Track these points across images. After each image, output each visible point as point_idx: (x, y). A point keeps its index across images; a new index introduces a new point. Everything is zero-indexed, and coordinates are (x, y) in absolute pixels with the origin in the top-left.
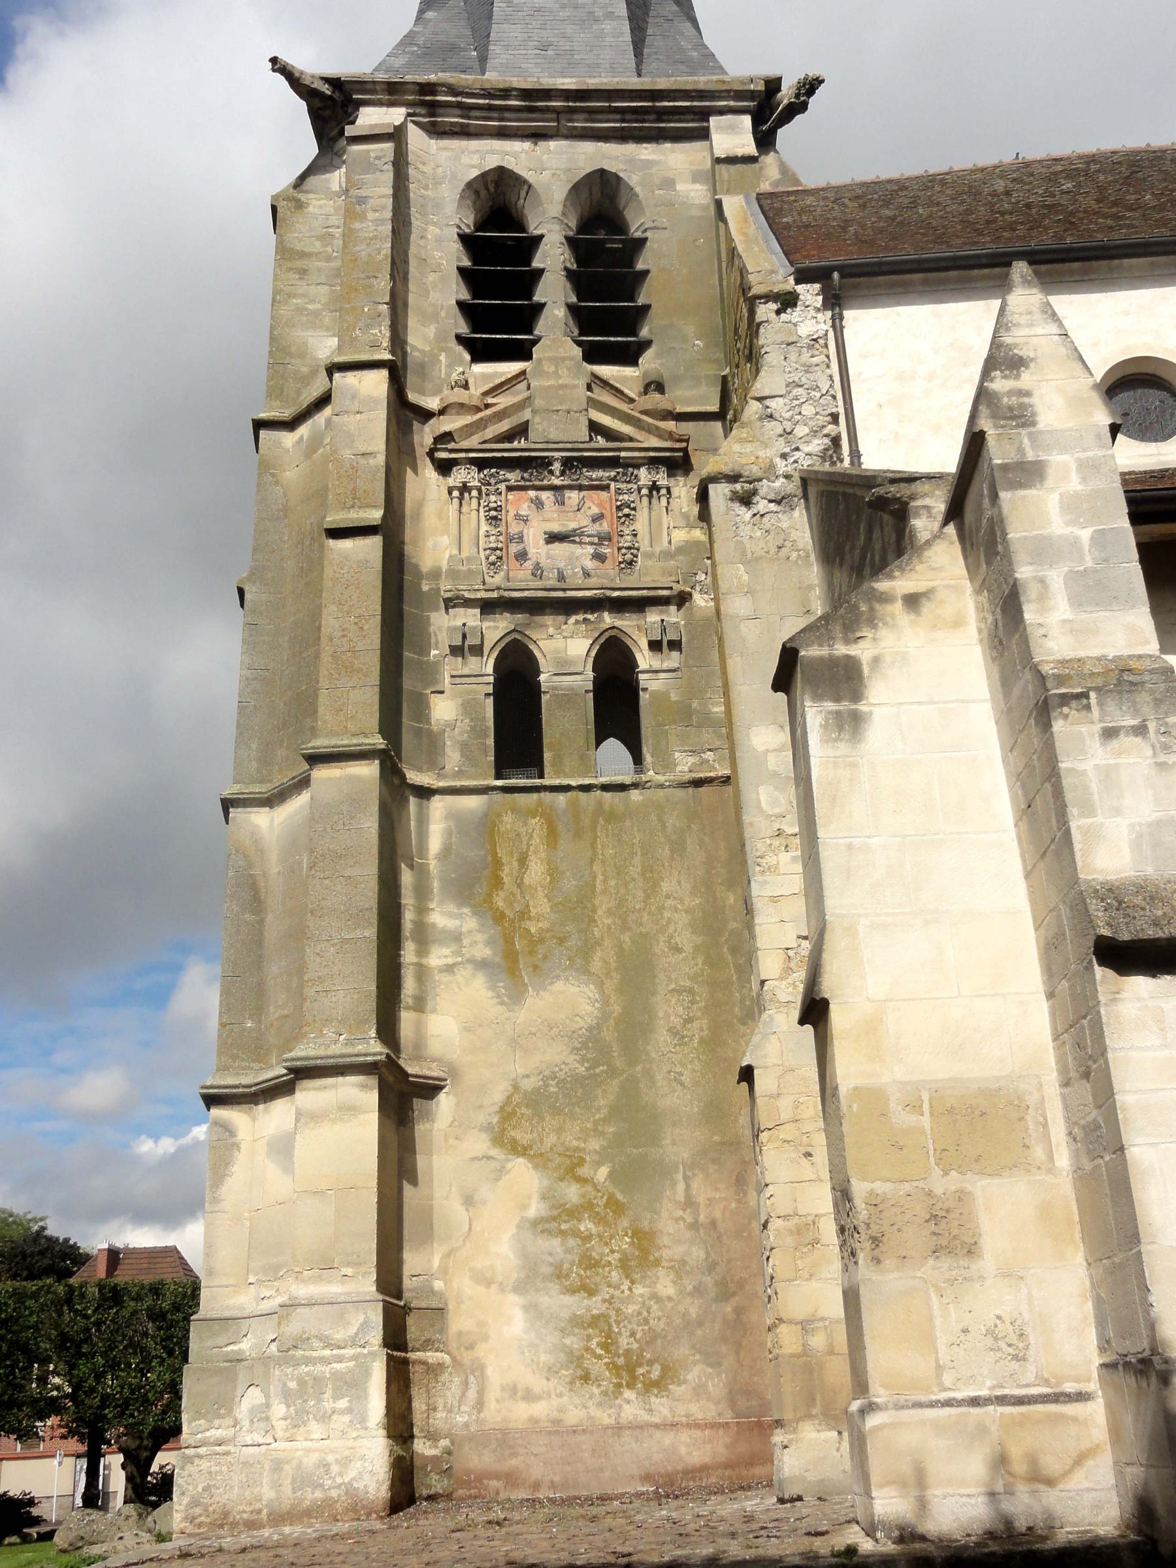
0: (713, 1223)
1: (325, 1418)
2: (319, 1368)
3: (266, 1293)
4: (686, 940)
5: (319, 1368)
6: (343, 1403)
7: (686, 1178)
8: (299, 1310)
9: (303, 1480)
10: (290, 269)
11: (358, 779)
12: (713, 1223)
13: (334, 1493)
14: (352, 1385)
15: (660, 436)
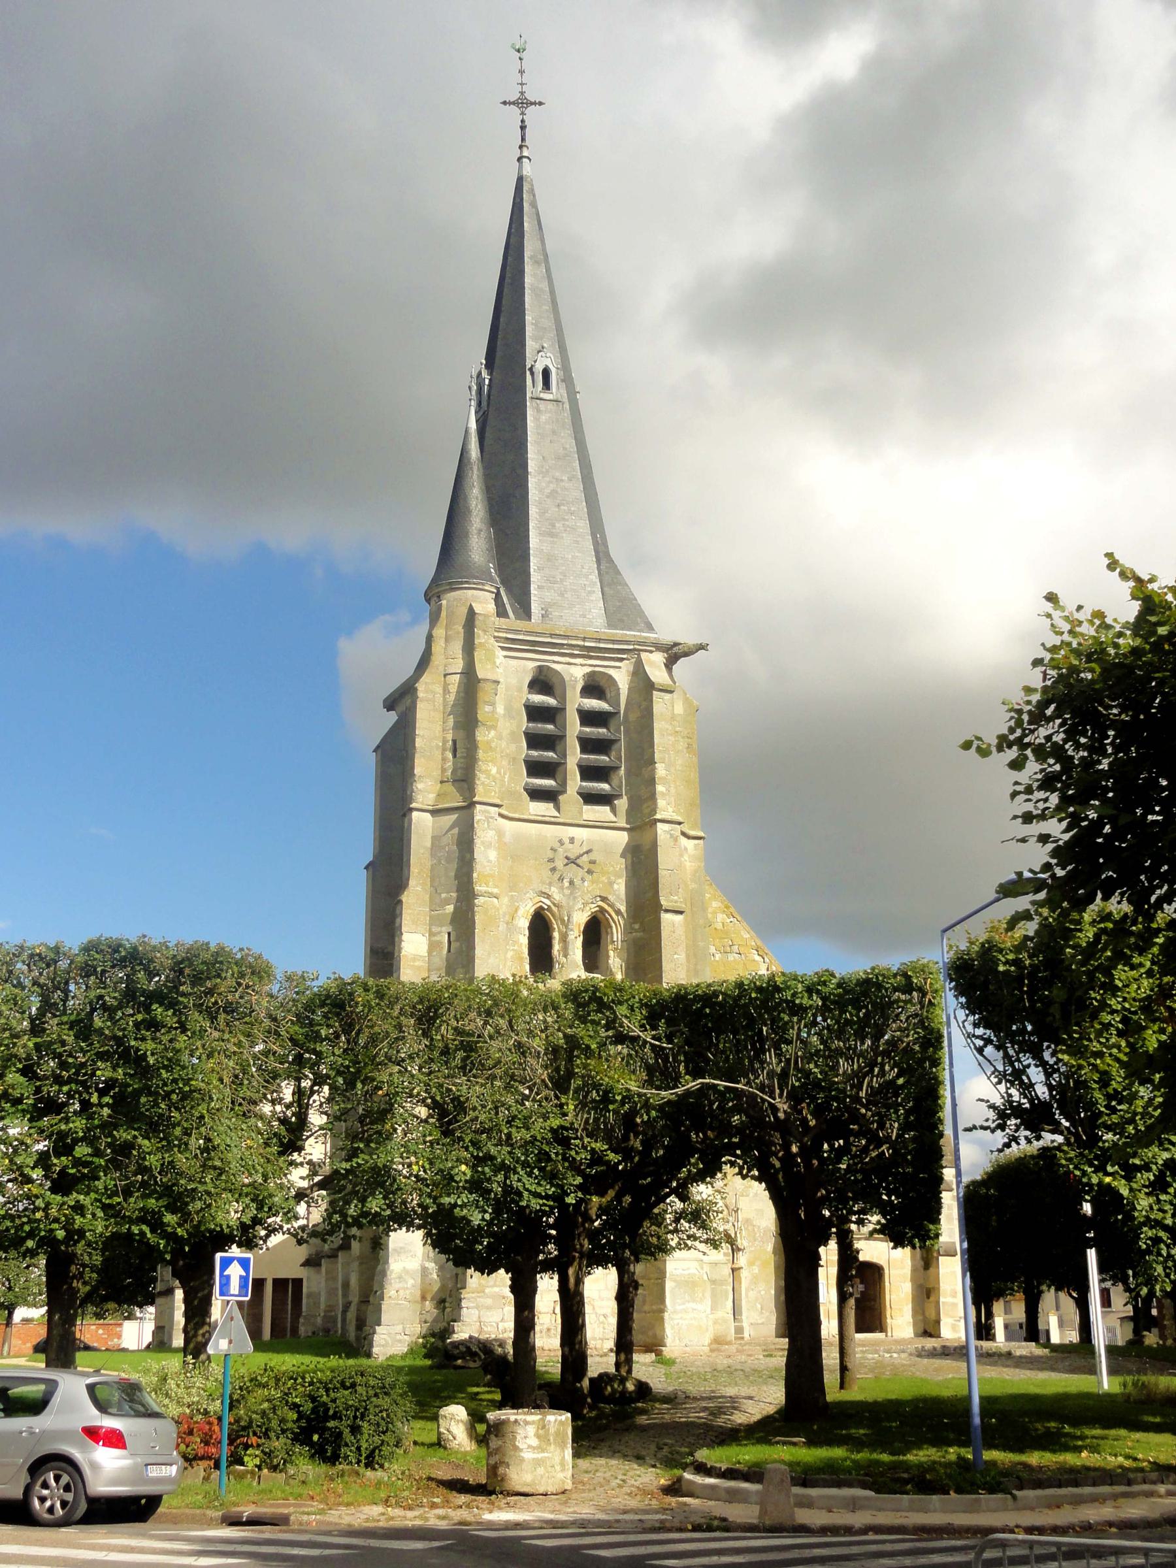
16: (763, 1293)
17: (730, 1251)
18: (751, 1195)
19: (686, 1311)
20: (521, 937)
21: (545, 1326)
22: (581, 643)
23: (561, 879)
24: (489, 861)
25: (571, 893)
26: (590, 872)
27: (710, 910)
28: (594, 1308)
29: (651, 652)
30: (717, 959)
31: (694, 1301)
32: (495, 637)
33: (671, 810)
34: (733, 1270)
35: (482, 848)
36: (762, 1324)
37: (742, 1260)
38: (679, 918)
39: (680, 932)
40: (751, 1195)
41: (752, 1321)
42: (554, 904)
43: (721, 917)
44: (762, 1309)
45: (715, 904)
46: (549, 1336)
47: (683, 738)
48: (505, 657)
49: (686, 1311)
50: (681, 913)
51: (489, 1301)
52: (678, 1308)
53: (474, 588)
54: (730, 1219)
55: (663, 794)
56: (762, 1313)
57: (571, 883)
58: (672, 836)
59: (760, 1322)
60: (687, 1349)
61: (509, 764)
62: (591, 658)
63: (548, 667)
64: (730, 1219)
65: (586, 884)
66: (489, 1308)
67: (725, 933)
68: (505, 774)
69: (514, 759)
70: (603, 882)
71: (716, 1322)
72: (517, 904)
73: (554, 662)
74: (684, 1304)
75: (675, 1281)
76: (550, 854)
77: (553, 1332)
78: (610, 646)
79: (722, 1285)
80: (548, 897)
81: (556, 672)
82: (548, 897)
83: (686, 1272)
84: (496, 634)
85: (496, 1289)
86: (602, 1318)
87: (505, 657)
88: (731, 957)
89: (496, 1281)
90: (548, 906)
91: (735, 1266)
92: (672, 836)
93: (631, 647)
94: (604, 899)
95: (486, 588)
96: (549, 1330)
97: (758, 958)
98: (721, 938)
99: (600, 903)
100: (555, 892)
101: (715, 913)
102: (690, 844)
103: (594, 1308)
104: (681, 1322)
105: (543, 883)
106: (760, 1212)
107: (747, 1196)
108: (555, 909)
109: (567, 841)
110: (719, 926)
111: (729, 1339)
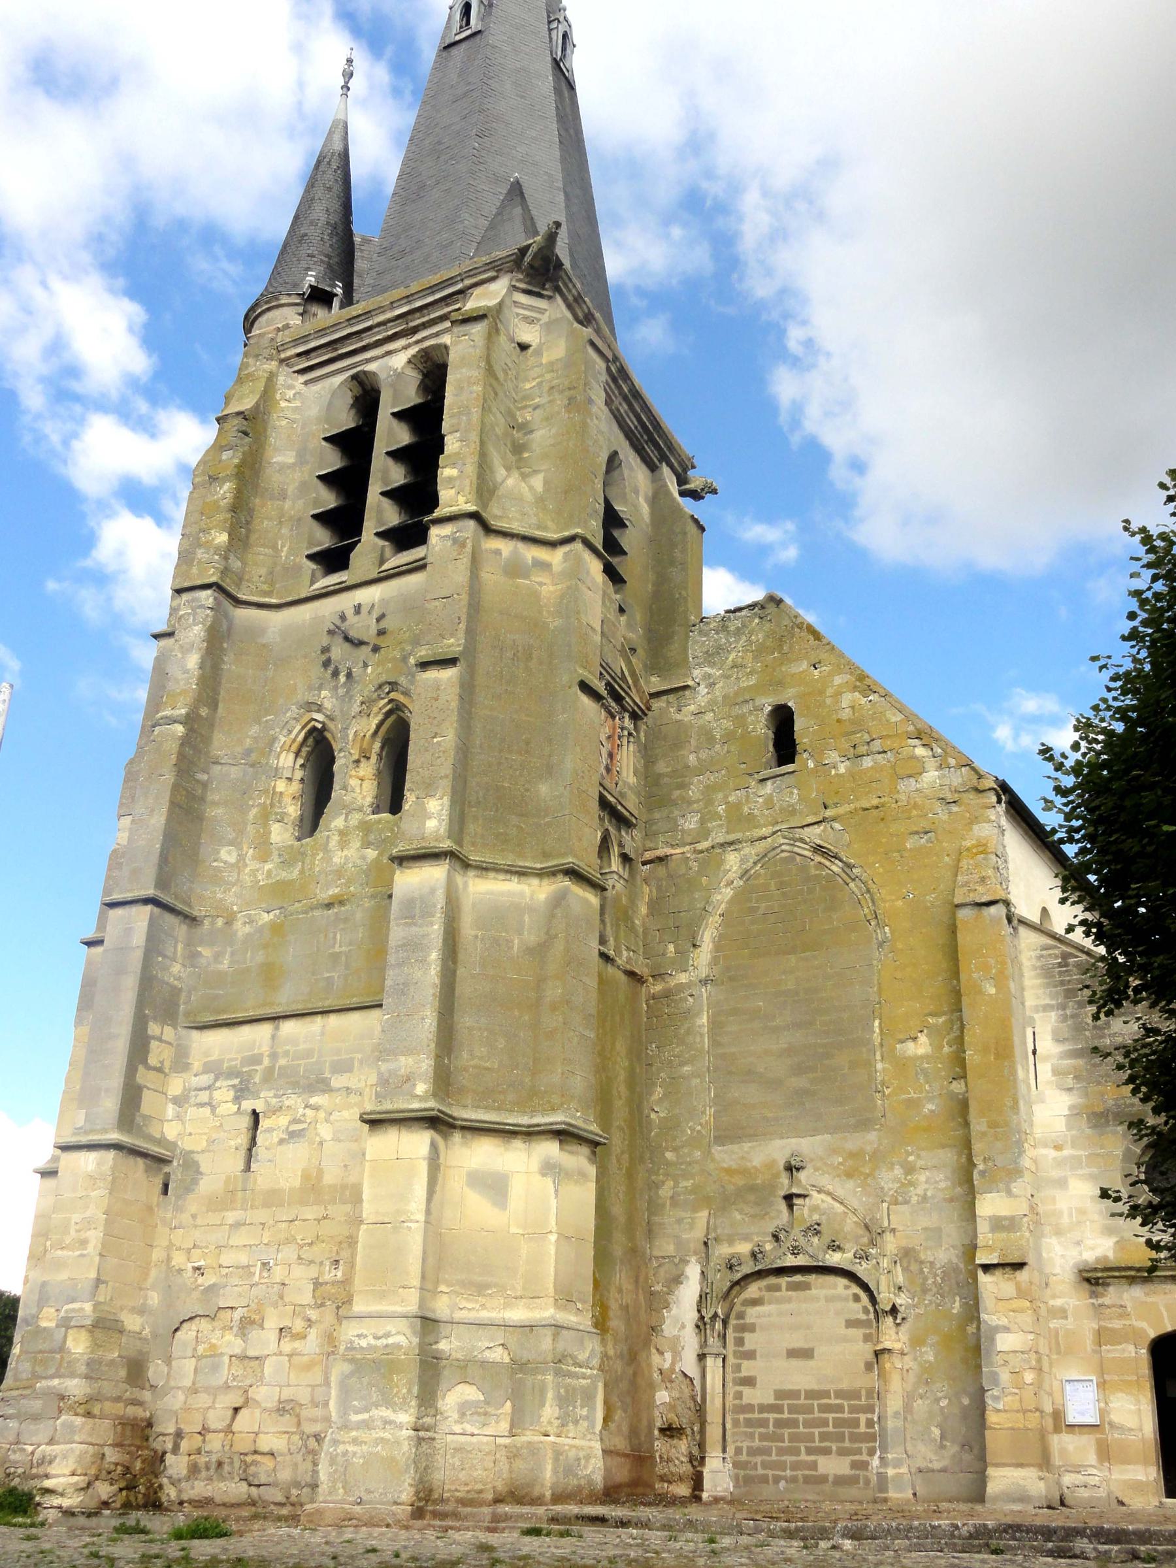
0: (627, 1306)
1: (576, 1422)
2: (574, 1382)
3: (463, 1304)
4: (623, 1089)
5: (574, 1382)
6: (584, 1412)
7: (620, 1271)
8: (564, 1332)
9: (569, 1471)
10: (491, 385)
11: (587, 901)
12: (627, 1306)
13: (583, 1482)
14: (589, 1398)
15: (641, 699)
16: (944, 1403)
17: (872, 1316)
18: (914, 1199)
19: (367, 1425)
20: (281, 786)
21: (214, 1458)
22: (389, 315)
23: (336, 674)
24: (186, 671)
25: (347, 692)
26: (376, 649)
27: (829, 692)
28: (299, 1424)
29: (493, 279)
30: (842, 770)
31: (388, 1403)
32: (282, 361)
33: (461, 499)
34: (877, 1354)
35: (180, 655)
36: (944, 1470)
37: (892, 1337)
38: (447, 675)
39: (450, 698)
40: (914, 1199)
41: (922, 1464)
42: (327, 716)
43: (847, 699)
44: (942, 1437)
45: (838, 680)
46: (222, 1478)
47: (562, 392)
48: (306, 383)
49: (367, 1425)
50: (451, 662)
51: (37, 1405)
52: (355, 1418)
53: (268, 309)
54: (873, 1251)
55: (450, 479)
56: (942, 1447)
57: (349, 675)
58: (455, 541)
59: (937, 1466)
60: (358, 1508)
61: (291, 530)
62: (415, 330)
63: (365, 372)
64: (873, 1251)
65: (369, 670)
66: (36, 1418)
67: (857, 724)
68: (283, 546)
69: (299, 520)
70: (394, 658)
71: (514, 1454)
72: (272, 732)
73: (368, 361)
74: (366, 1410)
75: (352, 1361)
76: (325, 640)
77: (226, 1468)
78: (430, 299)
79: (535, 1371)
80: (320, 709)
81: (374, 374)
82: (320, 709)
83: (384, 1341)
84: (283, 356)
85: (56, 1382)
86: (312, 1443)
87: (306, 383)
88: (867, 762)
89: (60, 1365)
90: (323, 723)
91: (879, 1348)
92: (455, 541)
93: (459, 286)
94: (394, 686)
95: (283, 302)
96: (220, 1464)
97: (920, 751)
98: (848, 734)
99: (393, 695)
100: (327, 698)
101: (838, 694)
102: (556, 557)
103: (299, 1424)
104: (351, 1448)
105: (310, 688)
106: (935, 1234)
107: (906, 1202)
108: (330, 725)
109: (349, 613)
110: (846, 714)
111: (536, 1492)
